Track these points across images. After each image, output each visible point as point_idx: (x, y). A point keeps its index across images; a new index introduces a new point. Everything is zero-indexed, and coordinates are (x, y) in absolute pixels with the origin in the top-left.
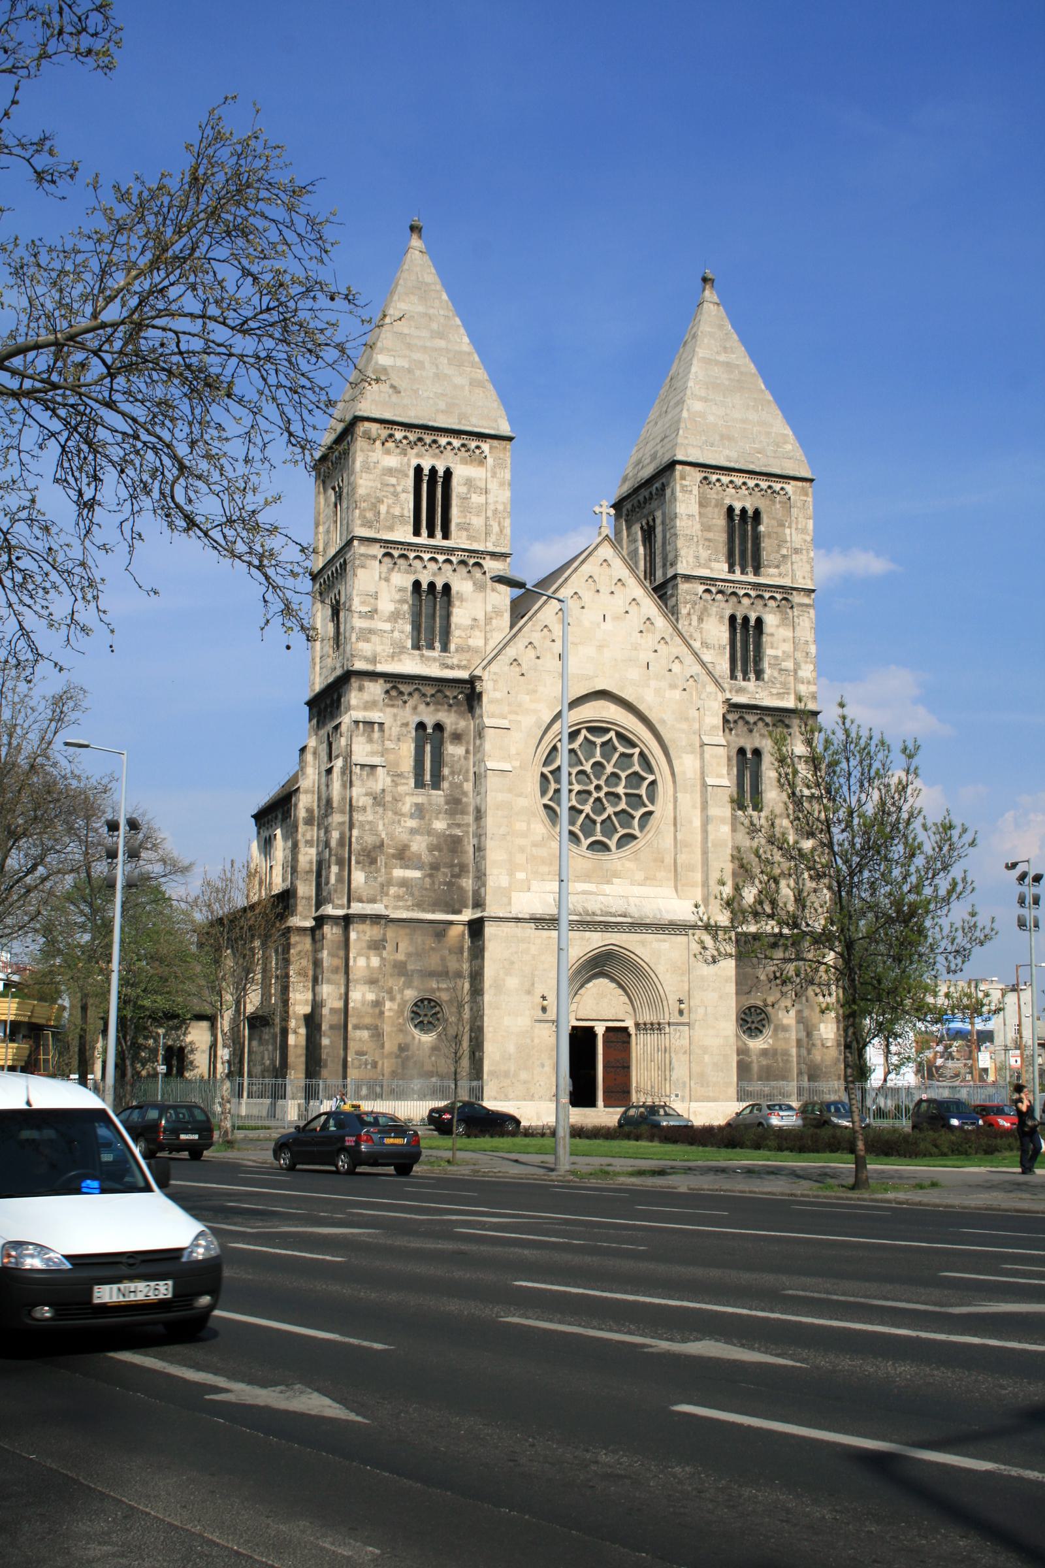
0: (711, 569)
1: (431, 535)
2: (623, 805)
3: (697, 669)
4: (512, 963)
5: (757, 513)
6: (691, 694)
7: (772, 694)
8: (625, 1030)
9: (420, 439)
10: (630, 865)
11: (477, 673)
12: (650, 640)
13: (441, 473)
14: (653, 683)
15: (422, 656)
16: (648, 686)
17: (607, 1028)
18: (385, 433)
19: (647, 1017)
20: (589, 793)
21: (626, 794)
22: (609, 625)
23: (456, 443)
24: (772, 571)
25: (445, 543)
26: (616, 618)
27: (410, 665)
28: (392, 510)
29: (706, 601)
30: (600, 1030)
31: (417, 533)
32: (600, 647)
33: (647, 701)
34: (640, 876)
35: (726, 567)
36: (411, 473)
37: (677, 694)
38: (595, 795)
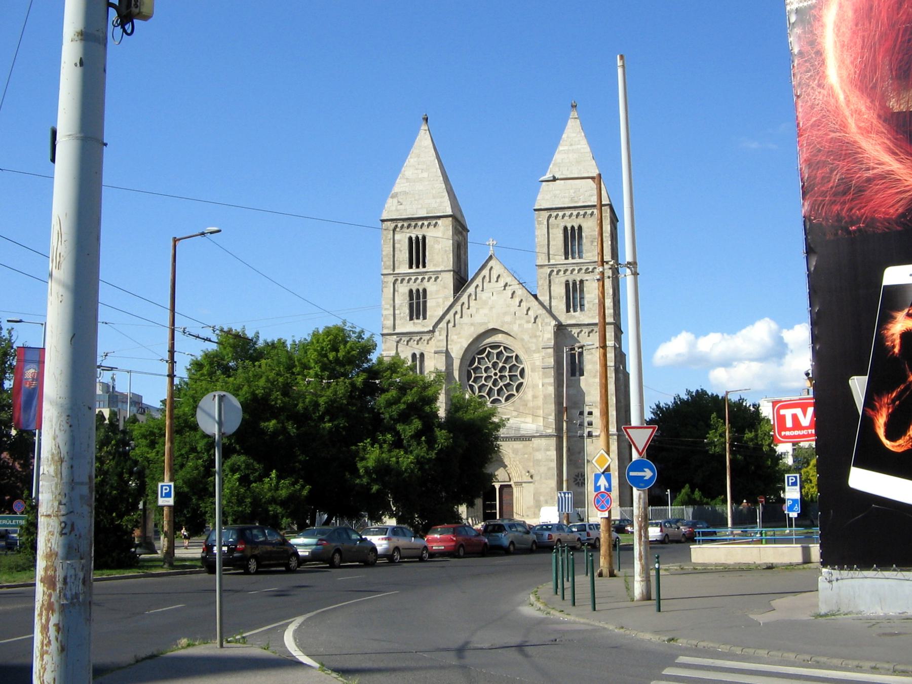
1: (418, 267)
2: (508, 381)
8: (510, 486)
13: (420, 237)
14: (518, 322)
18: (393, 225)
20: (491, 377)
25: (424, 270)
26: (499, 293)
31: (411, 267)
33: (514, 329)
36: (407, 241)
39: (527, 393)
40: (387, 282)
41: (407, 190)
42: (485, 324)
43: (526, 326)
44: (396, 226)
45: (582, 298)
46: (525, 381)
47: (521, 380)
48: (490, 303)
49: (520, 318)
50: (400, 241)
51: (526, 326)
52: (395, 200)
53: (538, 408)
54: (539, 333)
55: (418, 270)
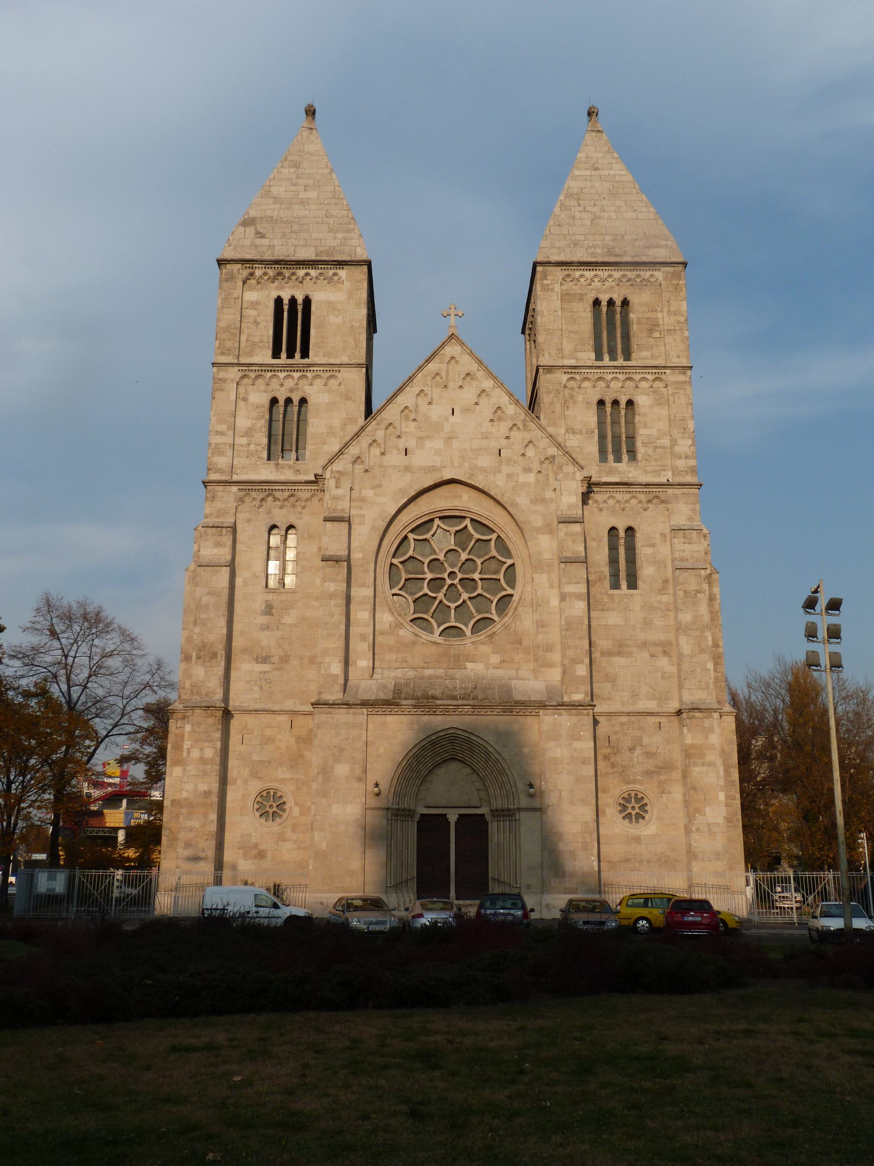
0: (576, 359)
1: (290, 355)
3: (553, 451)
4: (342, 750)
5: (625, 303)
6: (547, 475)
7: (646, 472)
9: (279, 274)
10: (486, 649)
11: (320, 472)
12: (503, 428)
13: (300, 299)
14: (505, 469)
15: (277, 464)
16: (500, 472)
17: (460, 815)
18: (245, 273)
19: (498, 804)
21: (481, 579)
22: (457, 418)
23: (313, 273)
24: (645, 354)
26: (466, 410)
27: (266, 472)
28: (251, 339)
29: (572, 389)
30: (453, 817)
31: (276, 354)
32: (449, 439)
33: (498, 484)
34: (495, 659)
35: (593, 355)
36: (271, 305)
37: (531, 478)
38: (449, 582)
39: (524, 620)
40: (224, 380)
41: (275, 214)
42: (433, 469)
43: (523, 478)
44: (252, 274)
45: (631, 438)
46: (517, 593)
47: (510, 591)
48: (447, 428)
49: (509, 461)
50: (255, 305)
51: (523, 478)
52: (250, 231)
53: (549, 648)
54: (549, 494)
55: (290, 361)
